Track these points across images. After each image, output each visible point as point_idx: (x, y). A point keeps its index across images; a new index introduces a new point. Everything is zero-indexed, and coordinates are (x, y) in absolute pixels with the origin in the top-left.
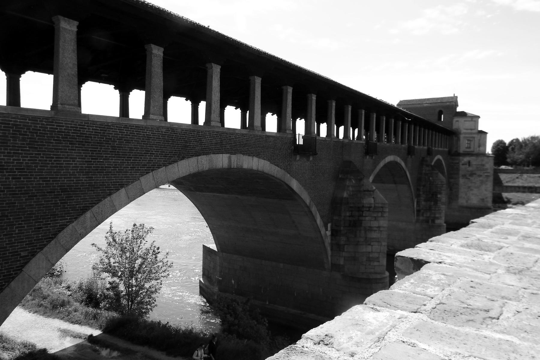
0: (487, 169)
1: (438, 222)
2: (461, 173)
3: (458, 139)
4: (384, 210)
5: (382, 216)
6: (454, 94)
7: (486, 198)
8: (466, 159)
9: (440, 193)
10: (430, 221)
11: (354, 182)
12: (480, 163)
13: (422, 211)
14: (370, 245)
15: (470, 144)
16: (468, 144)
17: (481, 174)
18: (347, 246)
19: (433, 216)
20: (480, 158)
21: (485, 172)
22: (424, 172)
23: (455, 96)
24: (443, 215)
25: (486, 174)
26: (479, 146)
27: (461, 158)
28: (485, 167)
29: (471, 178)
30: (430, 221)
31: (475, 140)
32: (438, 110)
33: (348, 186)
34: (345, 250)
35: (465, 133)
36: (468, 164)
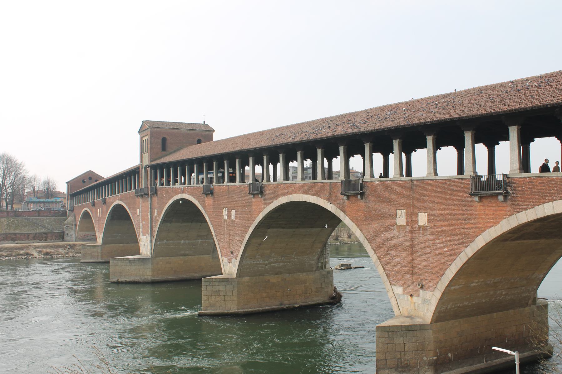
6: (204, 122)
23: (206, 123)
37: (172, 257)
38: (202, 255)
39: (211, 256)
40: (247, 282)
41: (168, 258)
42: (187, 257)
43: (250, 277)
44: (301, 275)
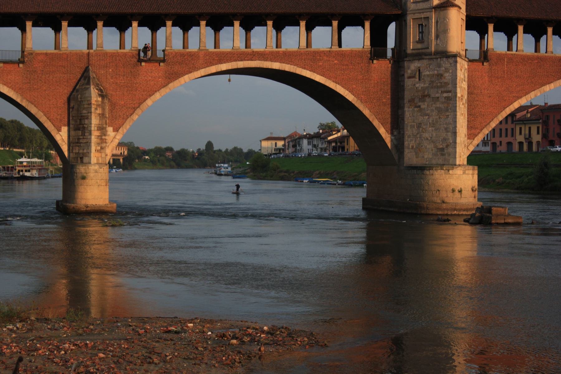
0: (446, 84)
2: (408, 95)
7: (447, 146)
8: (413, 66)
12: (436, 72)
17: (437, 95)
19: (81, 151)
21: (443, 89)
25: (445, 95)
36: (417, 76)
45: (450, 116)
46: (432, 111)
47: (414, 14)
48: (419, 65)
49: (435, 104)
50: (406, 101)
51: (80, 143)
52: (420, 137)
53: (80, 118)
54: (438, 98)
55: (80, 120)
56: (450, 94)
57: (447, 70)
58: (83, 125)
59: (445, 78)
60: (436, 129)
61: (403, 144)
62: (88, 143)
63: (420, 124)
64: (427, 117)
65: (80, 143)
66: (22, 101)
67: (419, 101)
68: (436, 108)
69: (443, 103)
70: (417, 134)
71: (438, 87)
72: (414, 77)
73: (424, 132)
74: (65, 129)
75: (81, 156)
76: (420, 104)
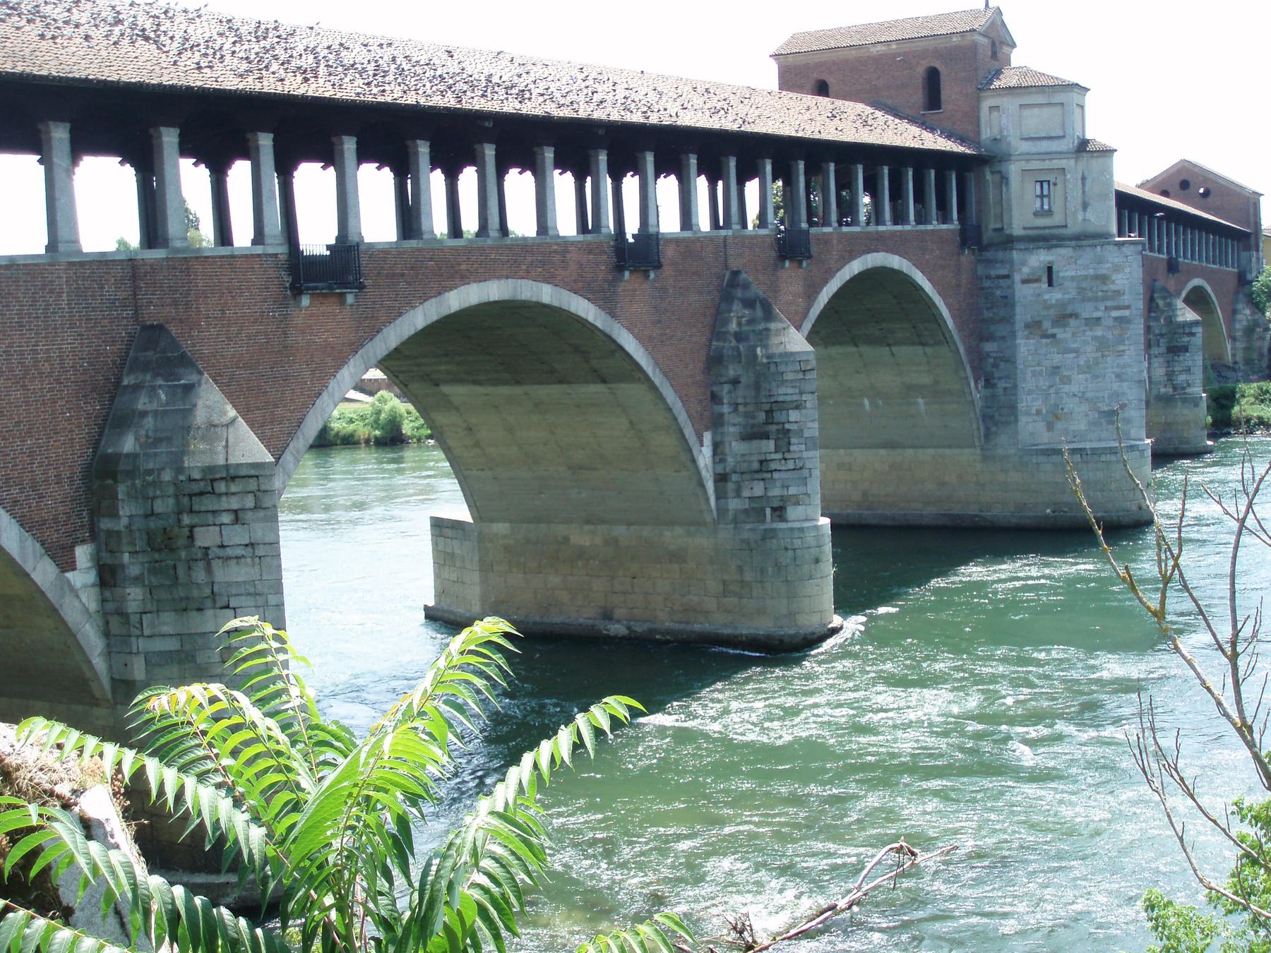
0: (1118, 293)
1: (793, 512)
2: (1022, 315)
3: (1004, 179)
4: (263, 487)
5: (257, 507)
7: (1123, 406)
8: (1038, 259)
9: (798, 406)
10: (768, 511)
11: (163, 397)
12: (1091, 272)
13: (735, 477)
14: (228, 607)
15: (1048, 196)
16: (1042, 196)
18: (148, 615)
19: (776, 492)
20: (1087, 255)
21: (1109, 304)
22: (733, 326)
24: (815, 487)
25: (1115, 314)
26: (1085, 206)
27: (1015, 255)
28: (1112, 287)
29: (1061, 334)
30: (768, 511)
31: (1065, 180)
32: (921, 70)
33: (144, 414)
34: (147, 632)
35: (1029, 156)
36: (1045, 279)
37: (854, 451)
38: (950, 447)
39: (978, 451)
40: (505, 537)
41: (842, 451)
42: (899, 451)
43: (510, 521)
44: (668, 534)
45: (1127, 353)
46: (1085, 342)
47: (1028, 160)
48: (1050, 258)
49: (1091, 330)
50: (1019, 325)
51: (771, 471)
52: (1056, 393)
53: (767, 407)
54: (1099, 319)
55: (769, 413)
56: (1126, 313)
57: (1117, 268)
58: (783, 423)
59: (1113, 282)
60: (1095, 377)
61: (1013, 407)
62: (805, 472)
63: (1058, 367)
64: (1072, 355)
65: (771, 471)
66: (654, 372)
67: (1053, 327)
68: (1094, 338)
69: (1109, 328)
70: (1051, 386)
71: (1096, 299)
72: (1038, 280)
73: (1065, 384)
74: (707, 437)
75: (776, 504)
76: (1055, 331)
